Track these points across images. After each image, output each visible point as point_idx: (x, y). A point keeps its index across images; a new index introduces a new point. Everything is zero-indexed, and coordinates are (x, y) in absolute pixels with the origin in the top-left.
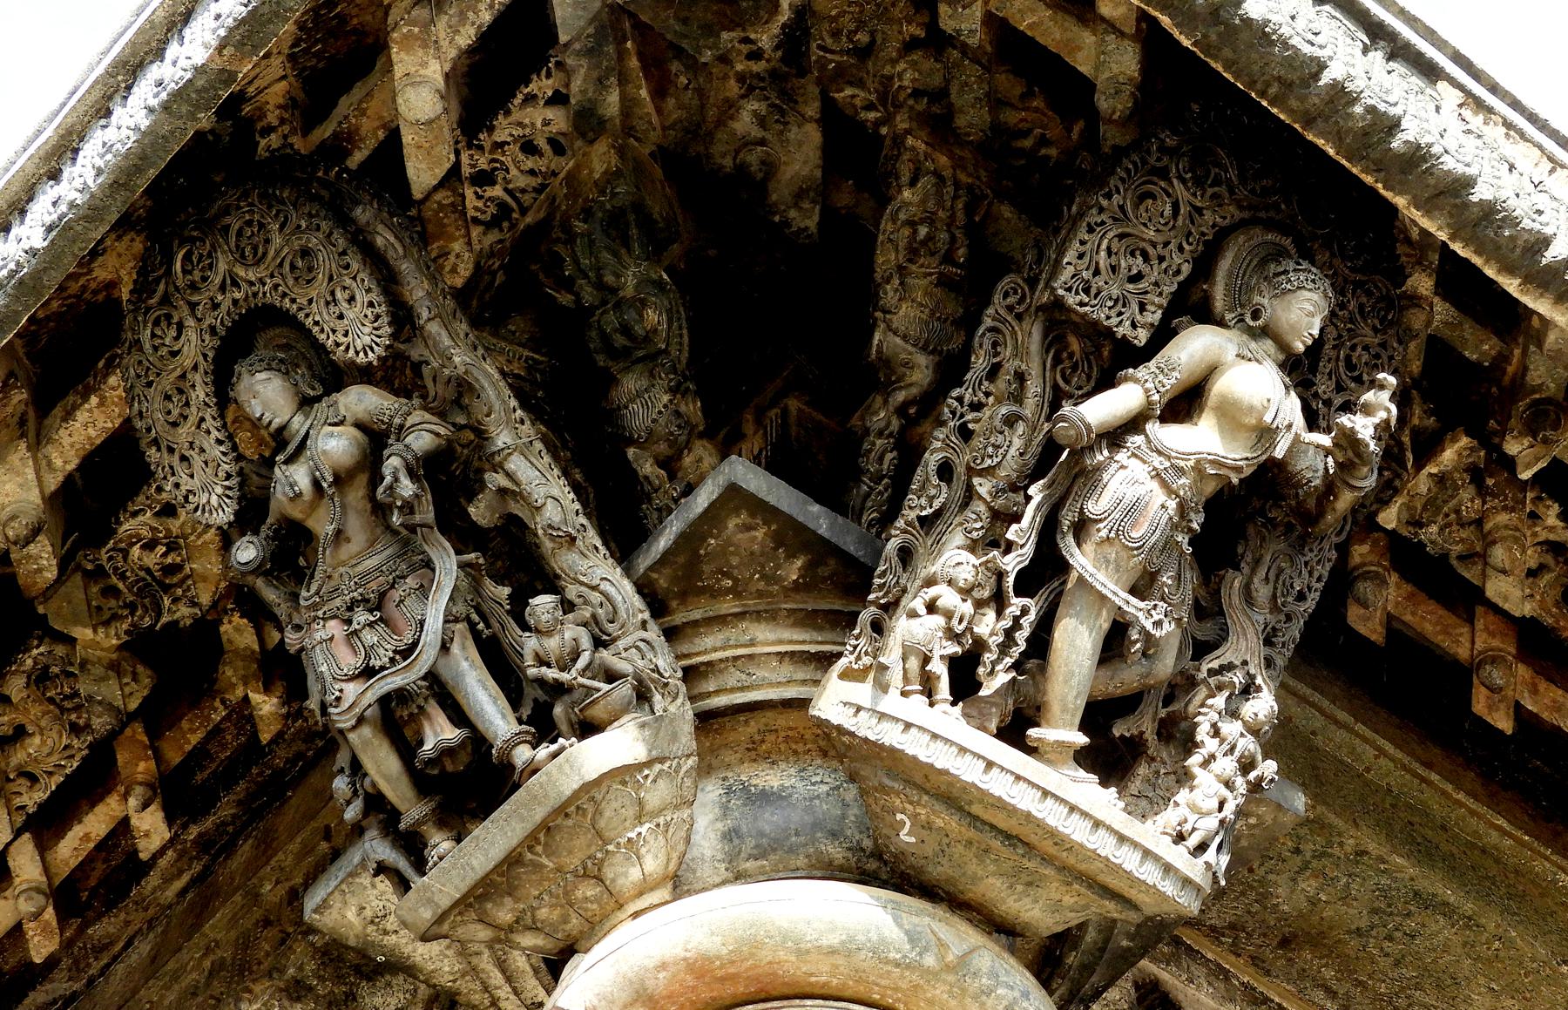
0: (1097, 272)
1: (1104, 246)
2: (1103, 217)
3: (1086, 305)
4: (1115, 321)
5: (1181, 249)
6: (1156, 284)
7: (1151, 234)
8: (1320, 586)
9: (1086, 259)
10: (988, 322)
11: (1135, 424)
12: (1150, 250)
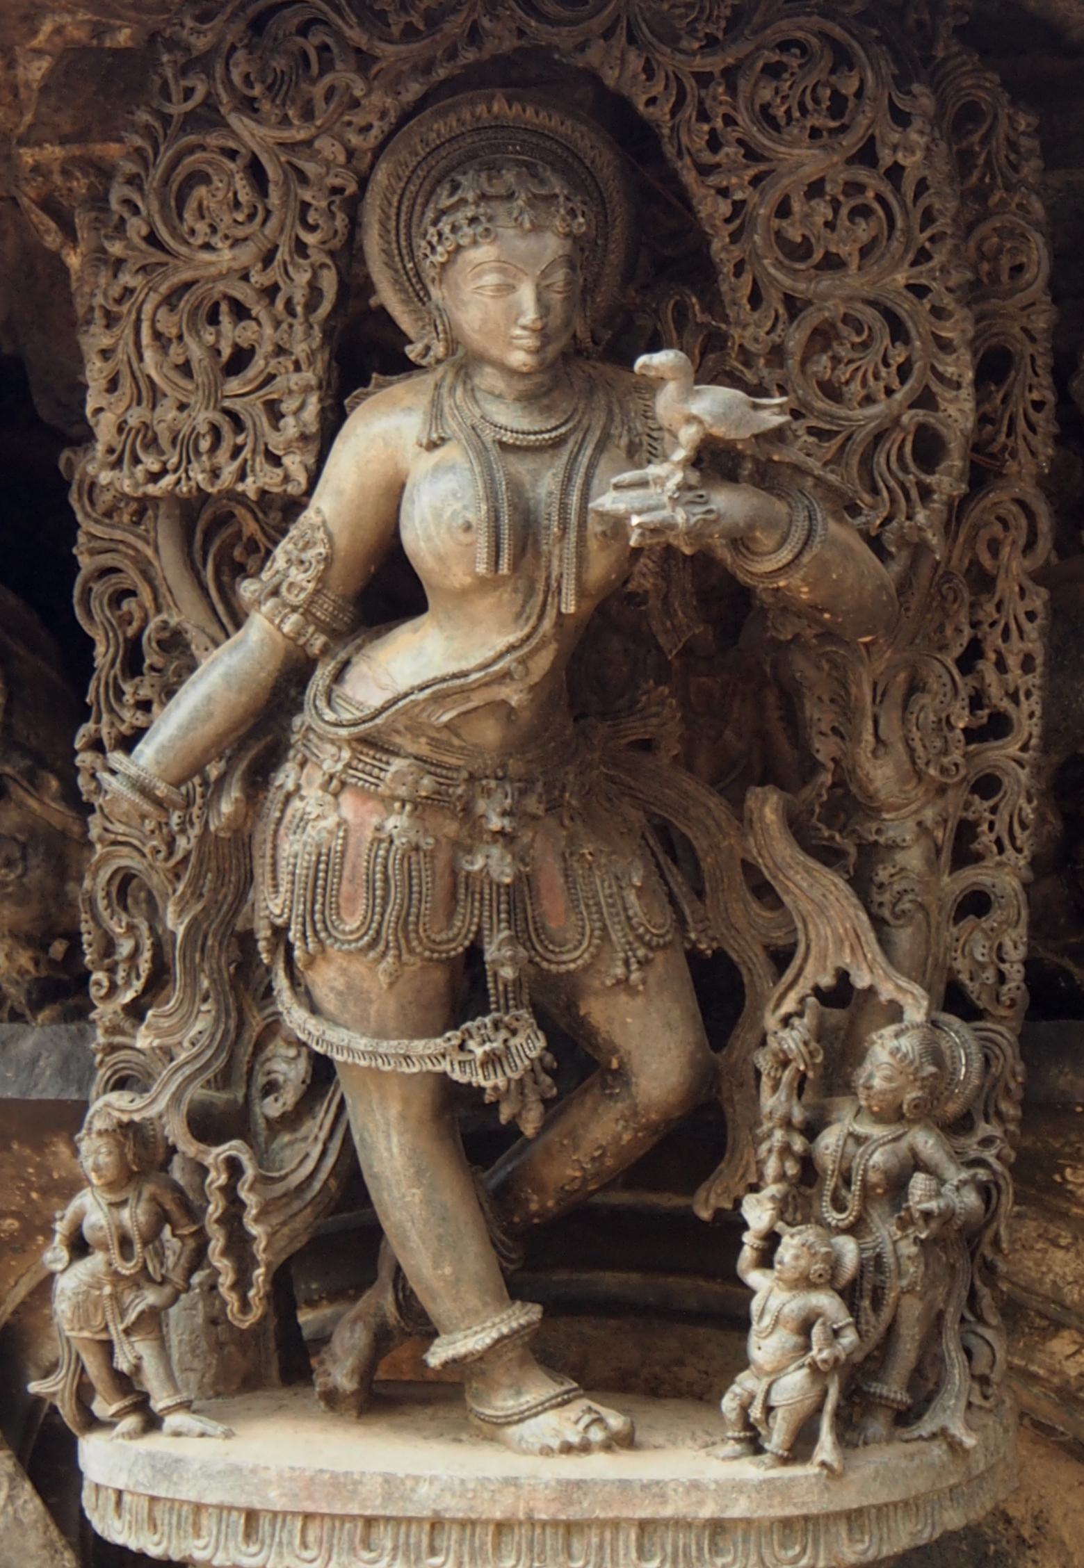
0: (156, 395)
1: (146, 337)
2: (126, 279)
3: (164, 472)
4: (229, 471)
5: (301, 248)
6: (280, 351)
7: (226, 257)
8: (1034, 679)
9: (126, 384)
10: (86, 563)
11: (287, 687)
12: (242, 292)
